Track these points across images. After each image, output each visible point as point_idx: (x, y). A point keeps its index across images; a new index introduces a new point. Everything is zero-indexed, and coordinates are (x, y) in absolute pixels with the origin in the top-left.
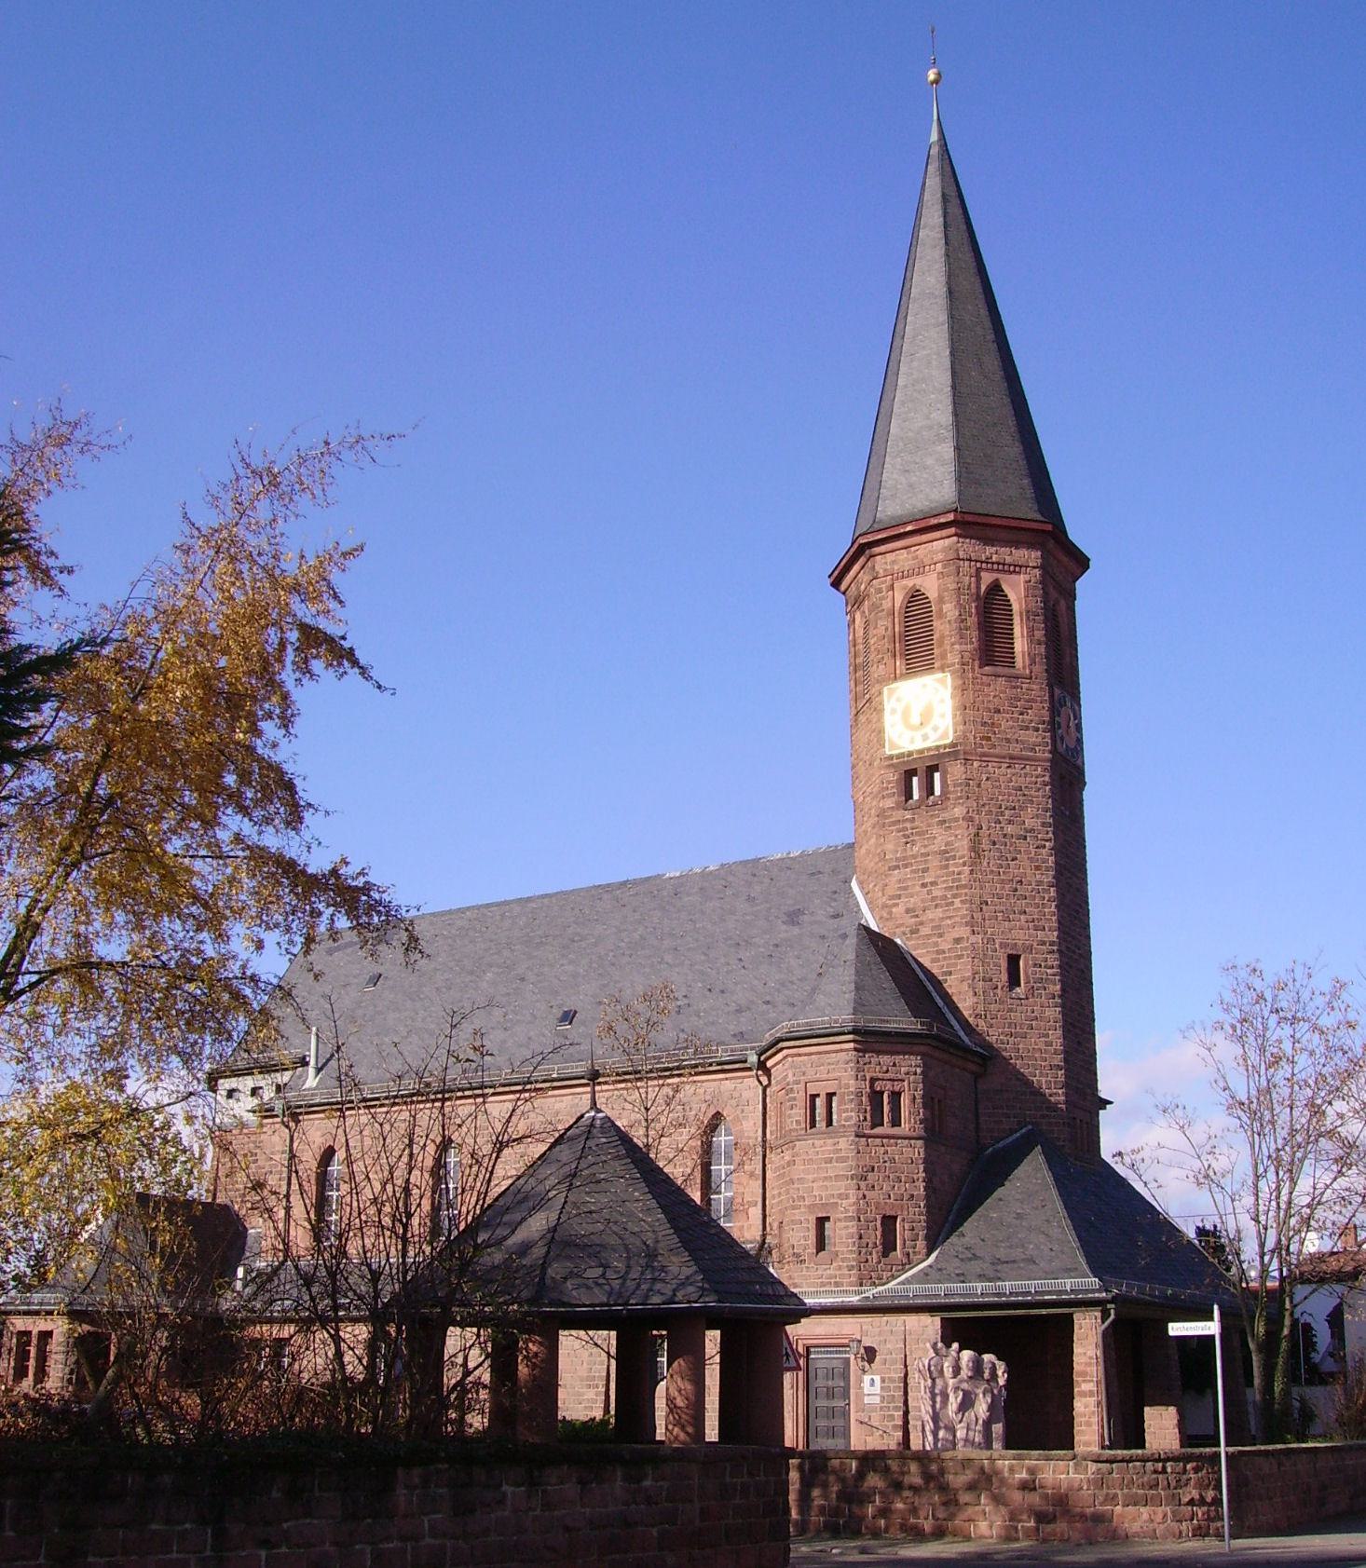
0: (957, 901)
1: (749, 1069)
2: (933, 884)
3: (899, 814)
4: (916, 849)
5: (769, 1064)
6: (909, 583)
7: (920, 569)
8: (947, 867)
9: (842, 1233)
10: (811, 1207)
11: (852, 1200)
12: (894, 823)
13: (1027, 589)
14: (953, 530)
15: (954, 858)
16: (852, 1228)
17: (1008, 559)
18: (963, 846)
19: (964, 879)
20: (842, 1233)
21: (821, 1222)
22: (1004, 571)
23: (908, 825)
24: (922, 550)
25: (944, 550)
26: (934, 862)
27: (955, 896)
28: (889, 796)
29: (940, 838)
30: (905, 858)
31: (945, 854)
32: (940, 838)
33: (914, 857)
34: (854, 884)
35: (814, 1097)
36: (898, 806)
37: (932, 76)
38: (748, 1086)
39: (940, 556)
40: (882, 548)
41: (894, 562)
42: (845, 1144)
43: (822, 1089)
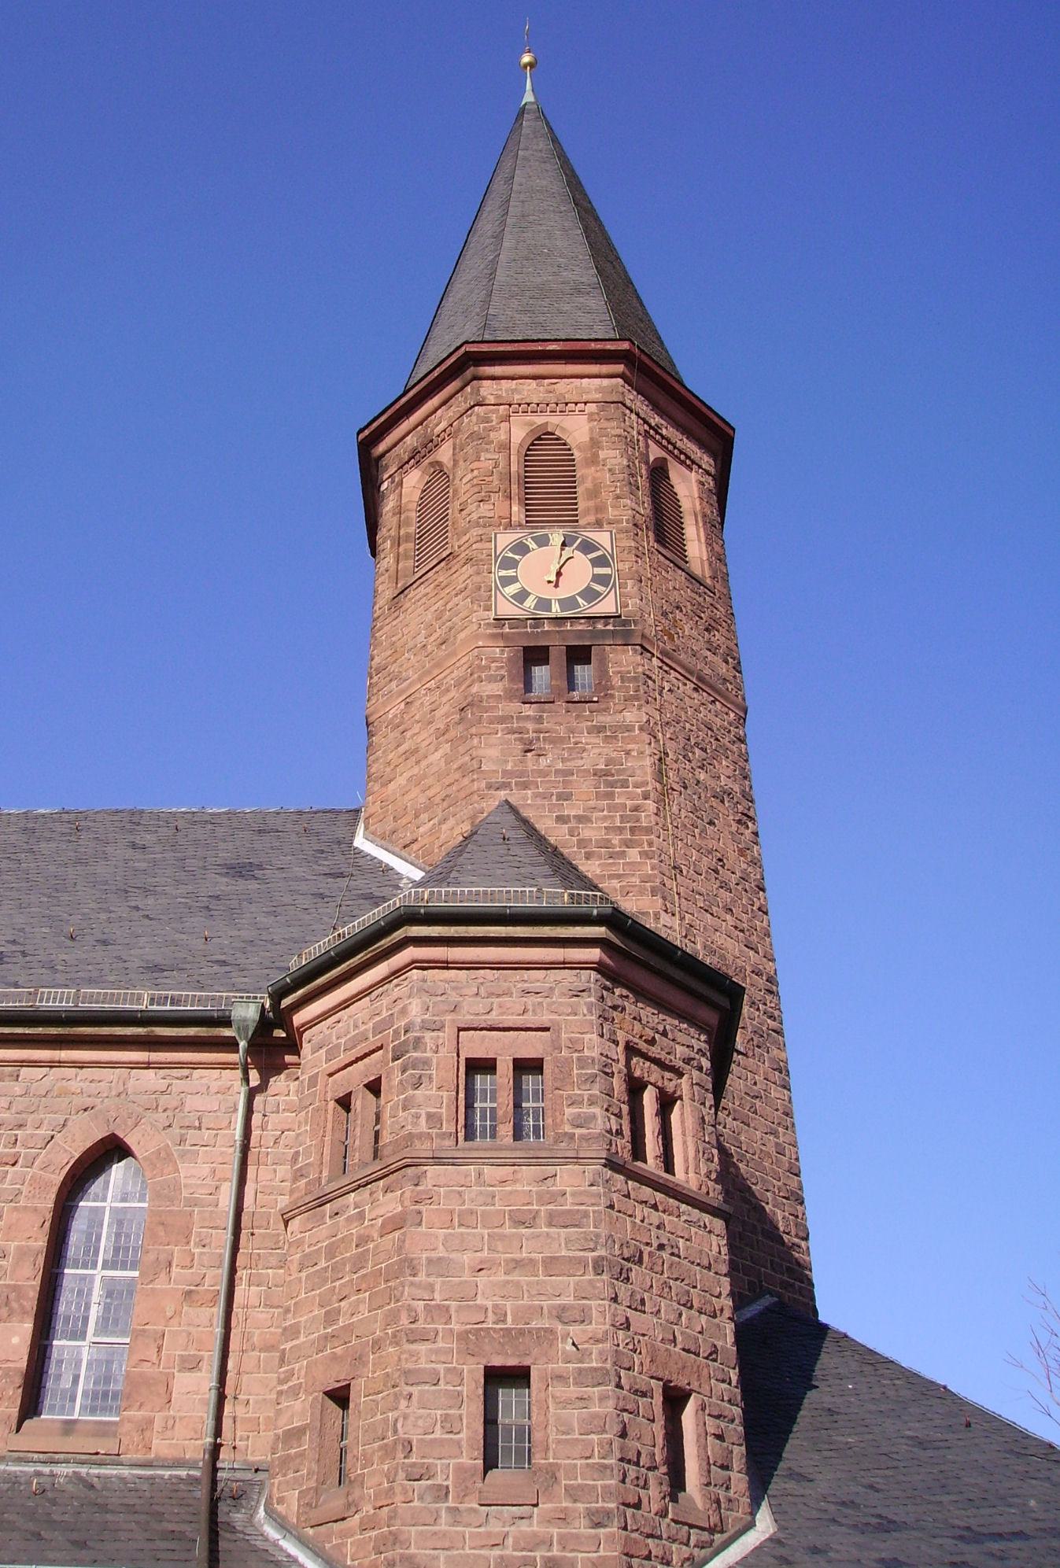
0: (633, 854)
1: (230, 1045)
2: (580, 819)
3: (515, 707)
4: (544, 762)
5: (298, 1019)
6: (539, 420)
7: (563, 406)
8: (610, 796)
9: (569, 1416)
10: (470, 1340)
11: (599, 1325)
12: (502, 720)
13: (701, 491)
14: (620, 368)
15: (624, 784)
16: (602, 1403)
17: (679, 444)
18: (642, 766)
19: (646, 819)
20: (569, 1416)
21: (504, 1378)
22: (677, 458)
23: (530, 726)
24: (562, 386)
25: (600, 390)
26: (584, 787)
27: (628, 844)
28: (491, 679)
29: (595, 753)
30: (522, 774)
31: (608, 778)
32: (595, 753)
33: (543, 773)
34: (360, 842)
35: (480, 1066)
36: (510, 696)
37: (526, 59)
38: (214, 1086)
39: (598, 396)
40: (497, 370)
41: (514, 391)
42: (577, 1182)
43: (505, 1049)
